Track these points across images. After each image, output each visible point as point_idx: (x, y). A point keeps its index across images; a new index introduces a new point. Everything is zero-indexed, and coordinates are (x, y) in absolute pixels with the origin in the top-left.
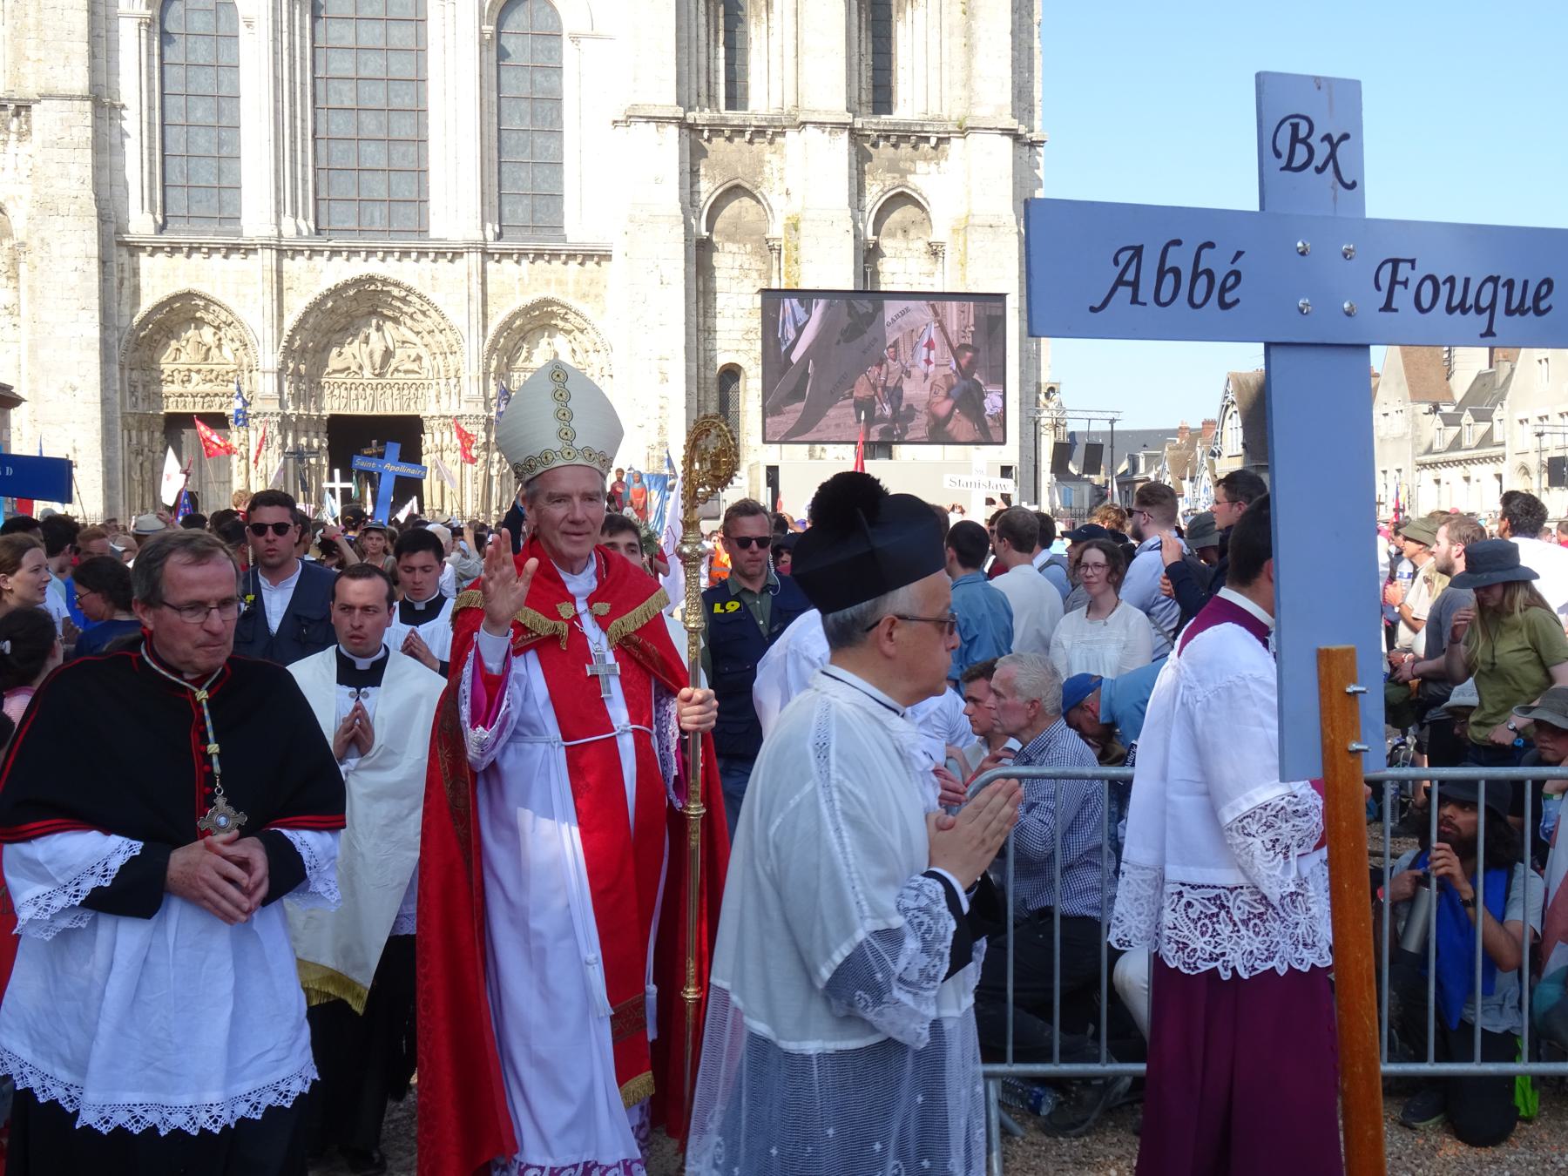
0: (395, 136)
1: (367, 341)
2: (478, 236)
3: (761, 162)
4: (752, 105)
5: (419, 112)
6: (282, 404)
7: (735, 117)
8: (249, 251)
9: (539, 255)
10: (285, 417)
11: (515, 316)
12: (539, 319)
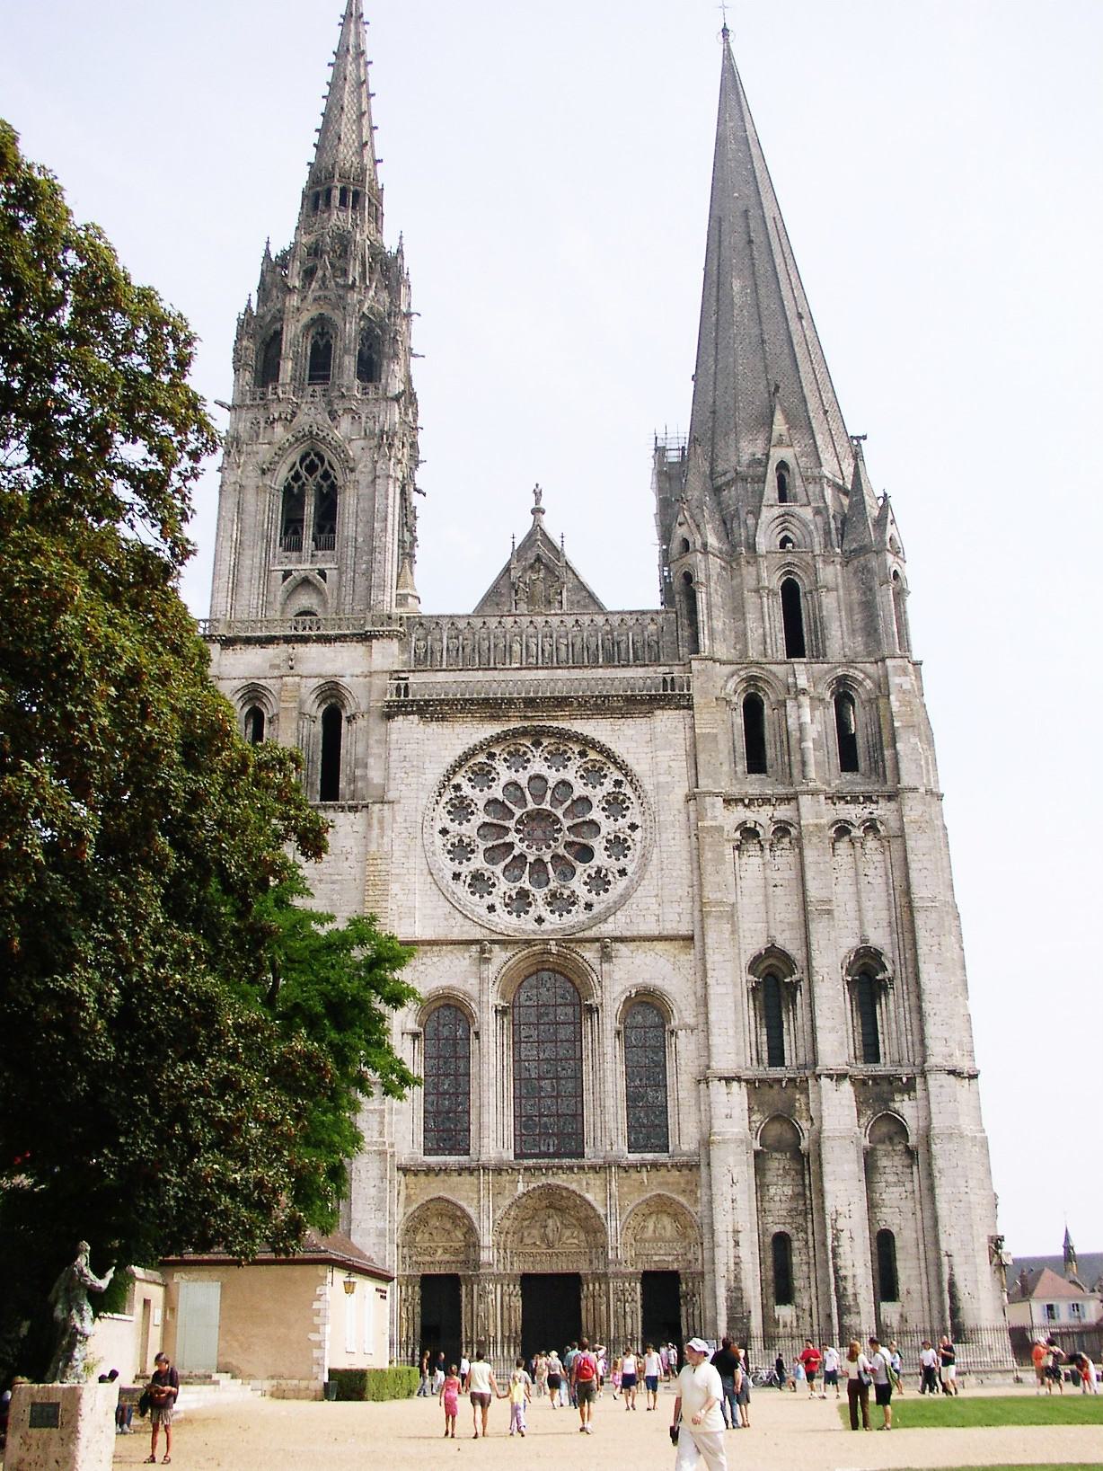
7: (776, 1072)
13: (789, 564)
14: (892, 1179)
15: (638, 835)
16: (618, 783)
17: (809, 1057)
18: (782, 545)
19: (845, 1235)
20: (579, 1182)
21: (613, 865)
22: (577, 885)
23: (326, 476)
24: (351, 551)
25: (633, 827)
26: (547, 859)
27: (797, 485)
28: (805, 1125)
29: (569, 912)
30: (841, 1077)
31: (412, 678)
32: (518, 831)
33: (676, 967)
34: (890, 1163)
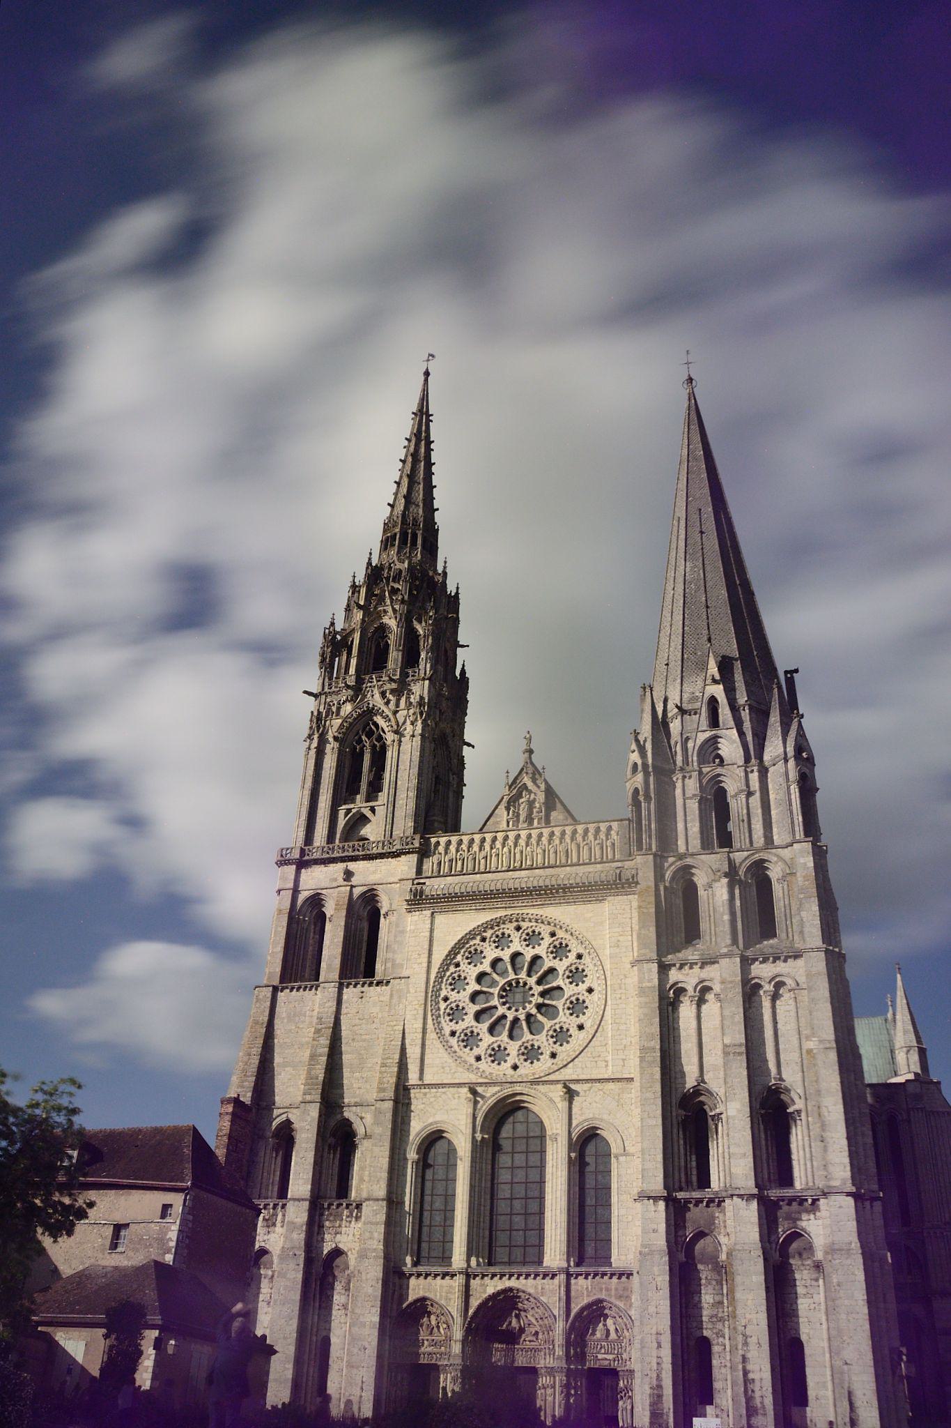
3: (713, 1218)
8: (453, 1276)
11: (583, 1309)
13: (719, 775)
19: (752, 1341)
20: (536, 1288)
22: (543, 1040)
23: (380, 738)
24: (392, 791)
25: (590, 990)
27: (725, 712)
28: (723, 1240)
29: (538, 1060)
30: (751, 1197)
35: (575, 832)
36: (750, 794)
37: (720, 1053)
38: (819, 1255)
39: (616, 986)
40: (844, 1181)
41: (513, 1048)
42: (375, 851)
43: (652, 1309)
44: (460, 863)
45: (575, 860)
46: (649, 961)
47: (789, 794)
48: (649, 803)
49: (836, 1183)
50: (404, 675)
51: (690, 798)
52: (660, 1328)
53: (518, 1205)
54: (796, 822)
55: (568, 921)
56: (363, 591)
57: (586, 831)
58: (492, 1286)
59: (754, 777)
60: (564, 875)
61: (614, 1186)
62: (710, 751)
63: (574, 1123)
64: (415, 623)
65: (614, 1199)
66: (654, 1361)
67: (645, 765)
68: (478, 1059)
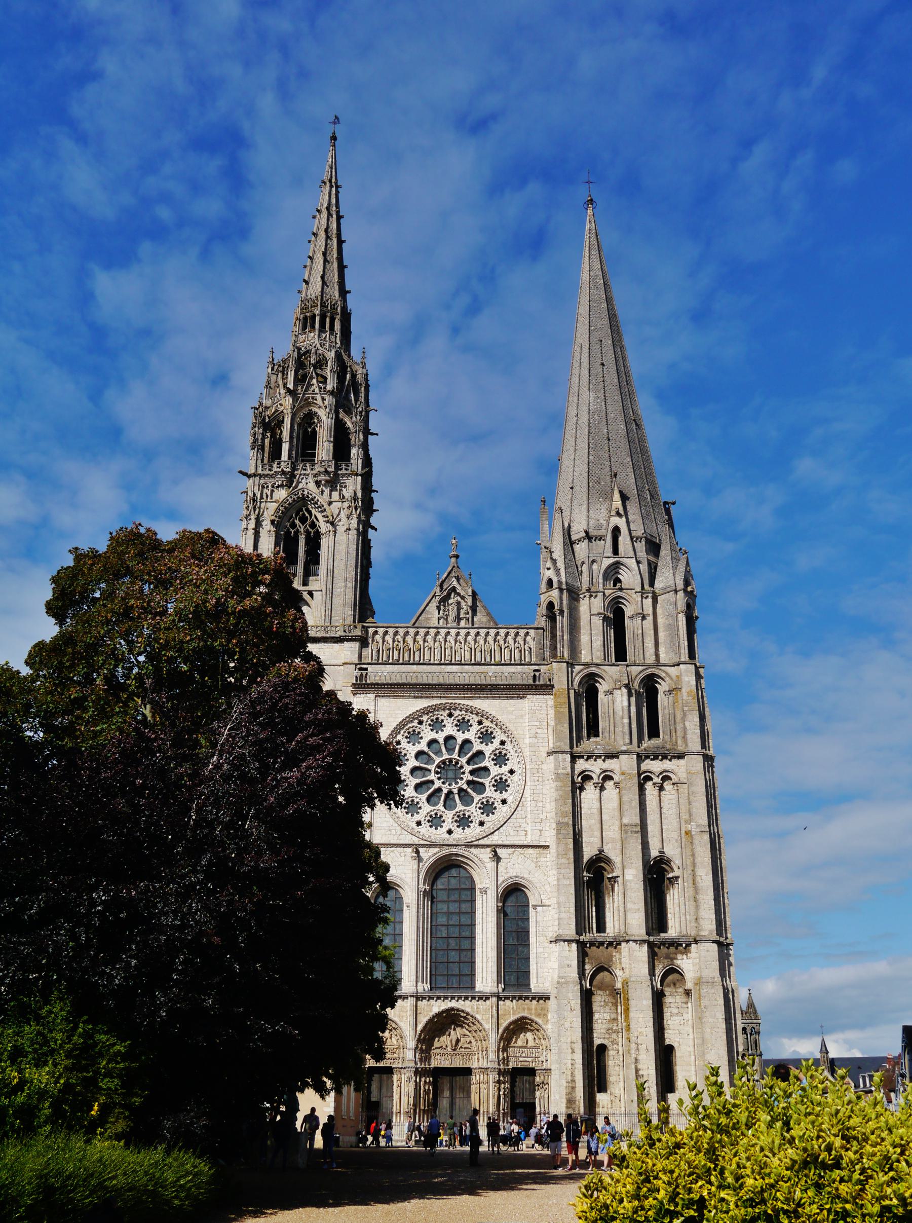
0: (462, 948)
1: (449, 1035)
2: (495, 990)
3: (612, 956)
4: (608, 930)
5: (472, 938)
6: (416, 1063)
7: (600, 937)
9: (520, 998)
10: (417, 1069)
11: (510, 1024)
12: (521, 1026)
14: (675, 1011)
15: (515, 777)
16: (503, 743)
17: (622, 928)
18: (615, 585)
19: (644, 1046)
20: (472, 1008)
21: (498, 797)
23: (313, 525)
24: (330, 578)
25: (512, 772)
26: (455, 791)
27: (624, 540)
28: (618, 973)
29: (469, 827)
31: (370, 668)
32: (437, 773)
33: (538, 866)
34: (672, 1000)
35: (497, 634)
36: (644, 618)
37: (616, 827)
38: (689, 985)
39: (535, 771)
40: (711, 932)
41: (449, 816)
42: (319, 635)
43: (567, 1025)
44: (396, 653)
45: (498, 659)
46: (563, 752)
47: (677, 621)
48: (563, 617)
49: (704, 933)
50: (338, 468)
51: (593, 615)
52: (574, 1039)
53: (452, 943)
54: (682, 646)
55: (494, 714)
56: (291, 375)
57: (507, 634)
58: (438, 1007)
59: (648, 602)
60: (491, 674)
61: (532, 930)
62: (612, 574)
63: (500, 880)
64: (342, 415)
65: (532, 940)
66: (570, 1062)
67: (560, 582)
68: (419, 823)
